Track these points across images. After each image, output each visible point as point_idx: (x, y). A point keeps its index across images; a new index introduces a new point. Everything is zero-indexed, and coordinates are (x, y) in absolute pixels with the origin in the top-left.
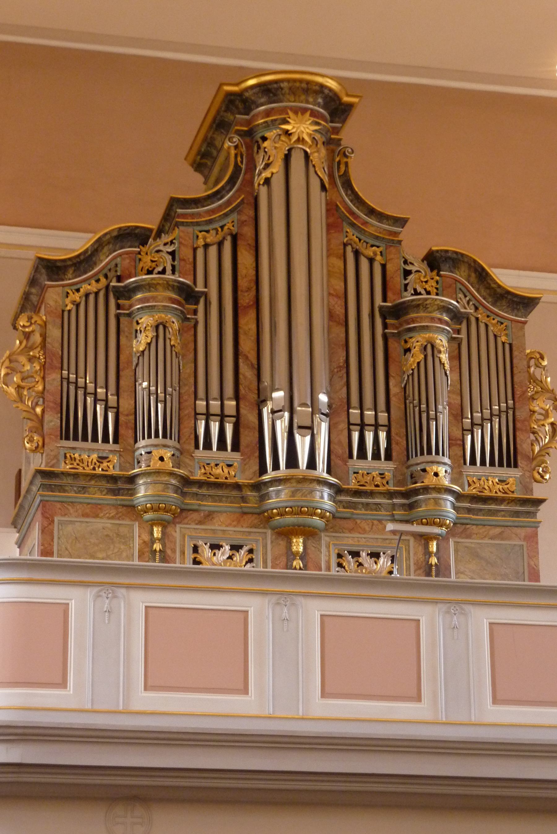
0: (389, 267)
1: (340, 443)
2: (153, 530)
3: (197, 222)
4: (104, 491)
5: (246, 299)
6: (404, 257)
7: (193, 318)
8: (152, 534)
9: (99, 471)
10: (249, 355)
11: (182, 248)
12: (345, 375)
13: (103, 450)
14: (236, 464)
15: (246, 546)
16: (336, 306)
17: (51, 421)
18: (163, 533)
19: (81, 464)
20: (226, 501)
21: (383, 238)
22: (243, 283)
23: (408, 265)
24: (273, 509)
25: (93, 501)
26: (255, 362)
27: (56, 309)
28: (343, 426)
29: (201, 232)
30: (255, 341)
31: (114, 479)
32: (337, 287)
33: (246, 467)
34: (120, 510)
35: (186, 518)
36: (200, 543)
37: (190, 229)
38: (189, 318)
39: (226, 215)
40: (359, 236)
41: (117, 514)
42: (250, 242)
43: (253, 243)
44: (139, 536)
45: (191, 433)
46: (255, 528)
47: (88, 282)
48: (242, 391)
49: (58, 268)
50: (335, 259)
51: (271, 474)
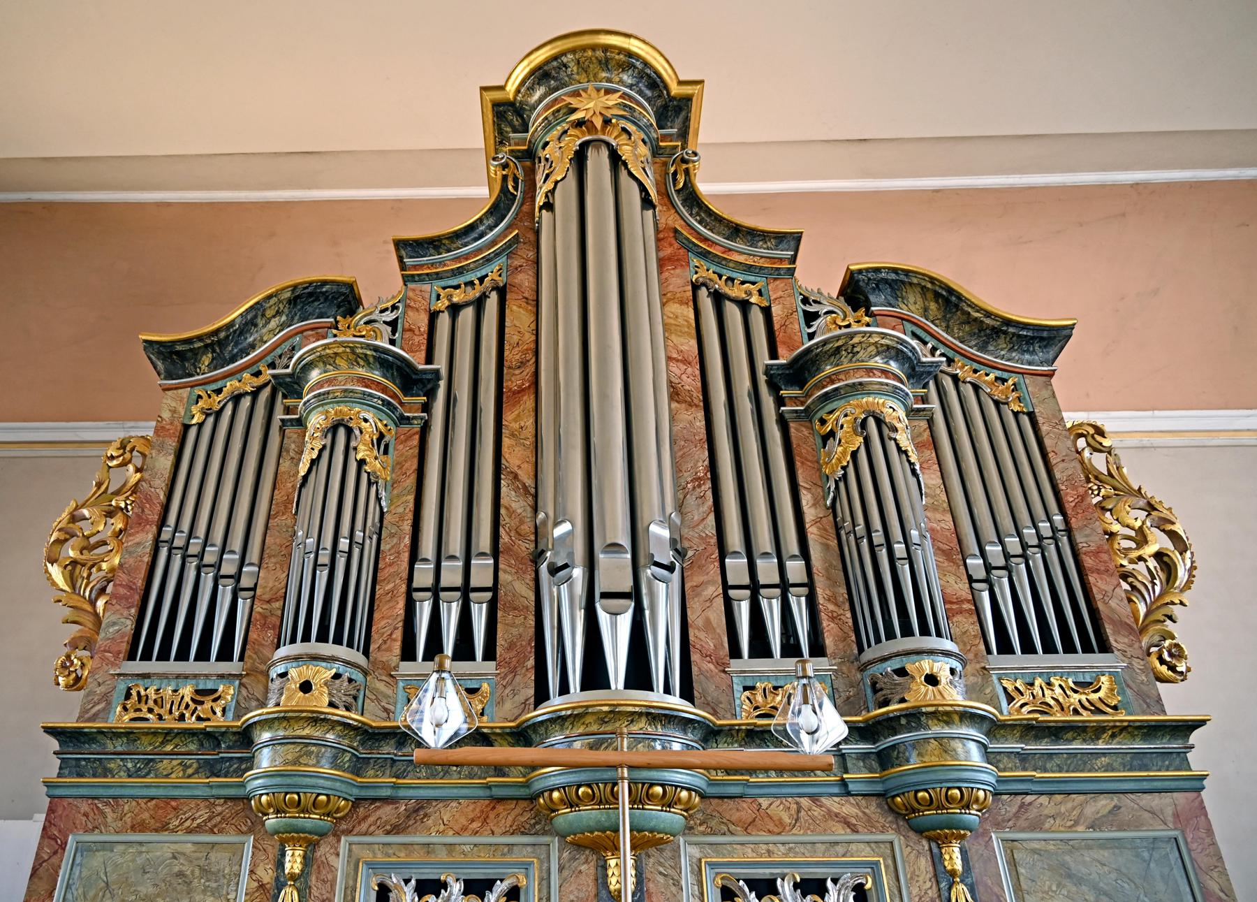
0: (776, 310)
1: (708, 625)
2: (283, 855)
3: (437, 273)
4: (190, 766)
6: (801, 294)
7: (414, 418)
8: (280, 864)
9: (191, 723)
10: (519, 472)
11: (410, 313)
12: (709, 494)
13: (207, 676)
14: (485, 686)
15: (502, 880)
16: (684, 377)
17: (114, 624)
18: (307, 862)
19: (156, 710)
20: (459, 773)
21: (761, 268)
23: (811, 305)
24: (552, 791)
25: (161, 792)
26: (529, 482)
27: (171, 424)
28: (715, 590)
29: (444, 288)
30: (532, 447)
31: (211, 738)
32: (684, 348)
33: (507, 691)
34: (219, 809)
35: (365, 818)
36: (394, 880)
37: (427, 287)
38: (408, 418)
39: (488, 260)
40: (718, 270)
41: (210, 819)
42: (526, 295)
43: (532, 297)
44: (252, 872)
45: (396, 628)
46: (523, 833)
47: (238, 376)
48: (504, 538)
49: (181, 354)
50: (677, 305)
51: (556, 703)
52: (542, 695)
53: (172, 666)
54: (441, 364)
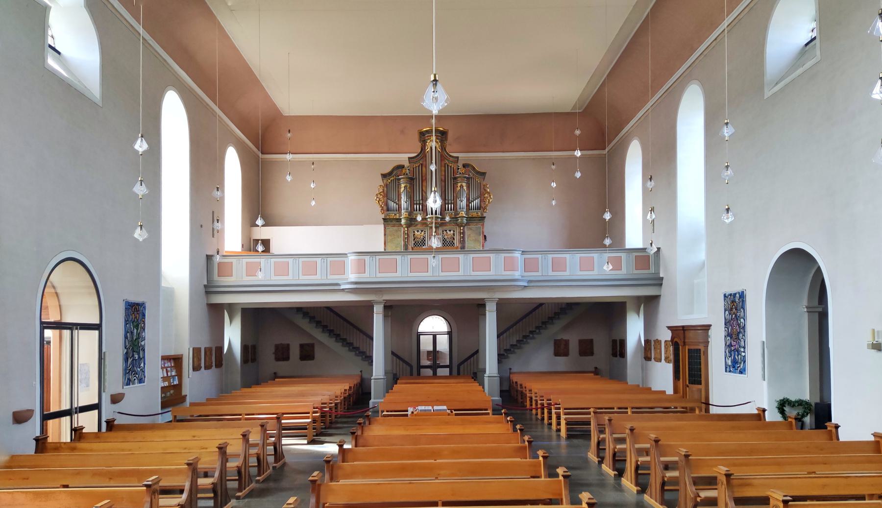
5: (424, 178)
22: (423, 175)
31: (397, 219)
51: (429, 216)
52: (427, 215)
53: (391, 212)
54: (415, 177)
